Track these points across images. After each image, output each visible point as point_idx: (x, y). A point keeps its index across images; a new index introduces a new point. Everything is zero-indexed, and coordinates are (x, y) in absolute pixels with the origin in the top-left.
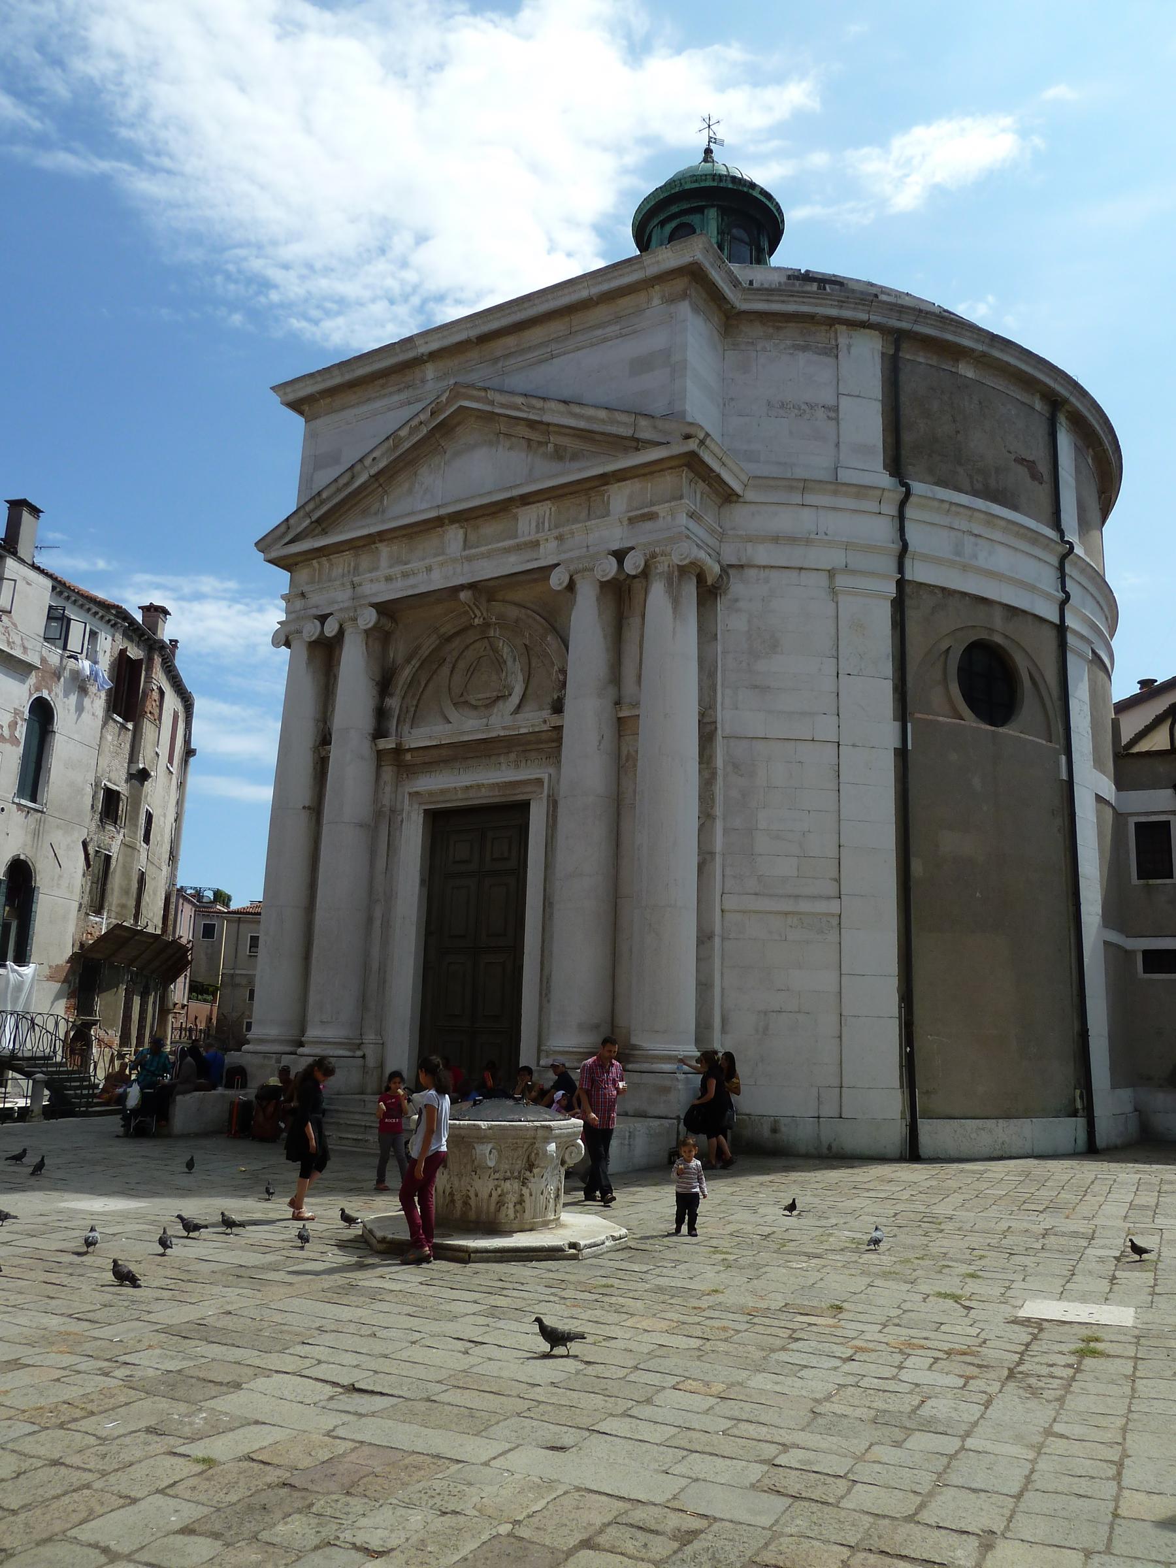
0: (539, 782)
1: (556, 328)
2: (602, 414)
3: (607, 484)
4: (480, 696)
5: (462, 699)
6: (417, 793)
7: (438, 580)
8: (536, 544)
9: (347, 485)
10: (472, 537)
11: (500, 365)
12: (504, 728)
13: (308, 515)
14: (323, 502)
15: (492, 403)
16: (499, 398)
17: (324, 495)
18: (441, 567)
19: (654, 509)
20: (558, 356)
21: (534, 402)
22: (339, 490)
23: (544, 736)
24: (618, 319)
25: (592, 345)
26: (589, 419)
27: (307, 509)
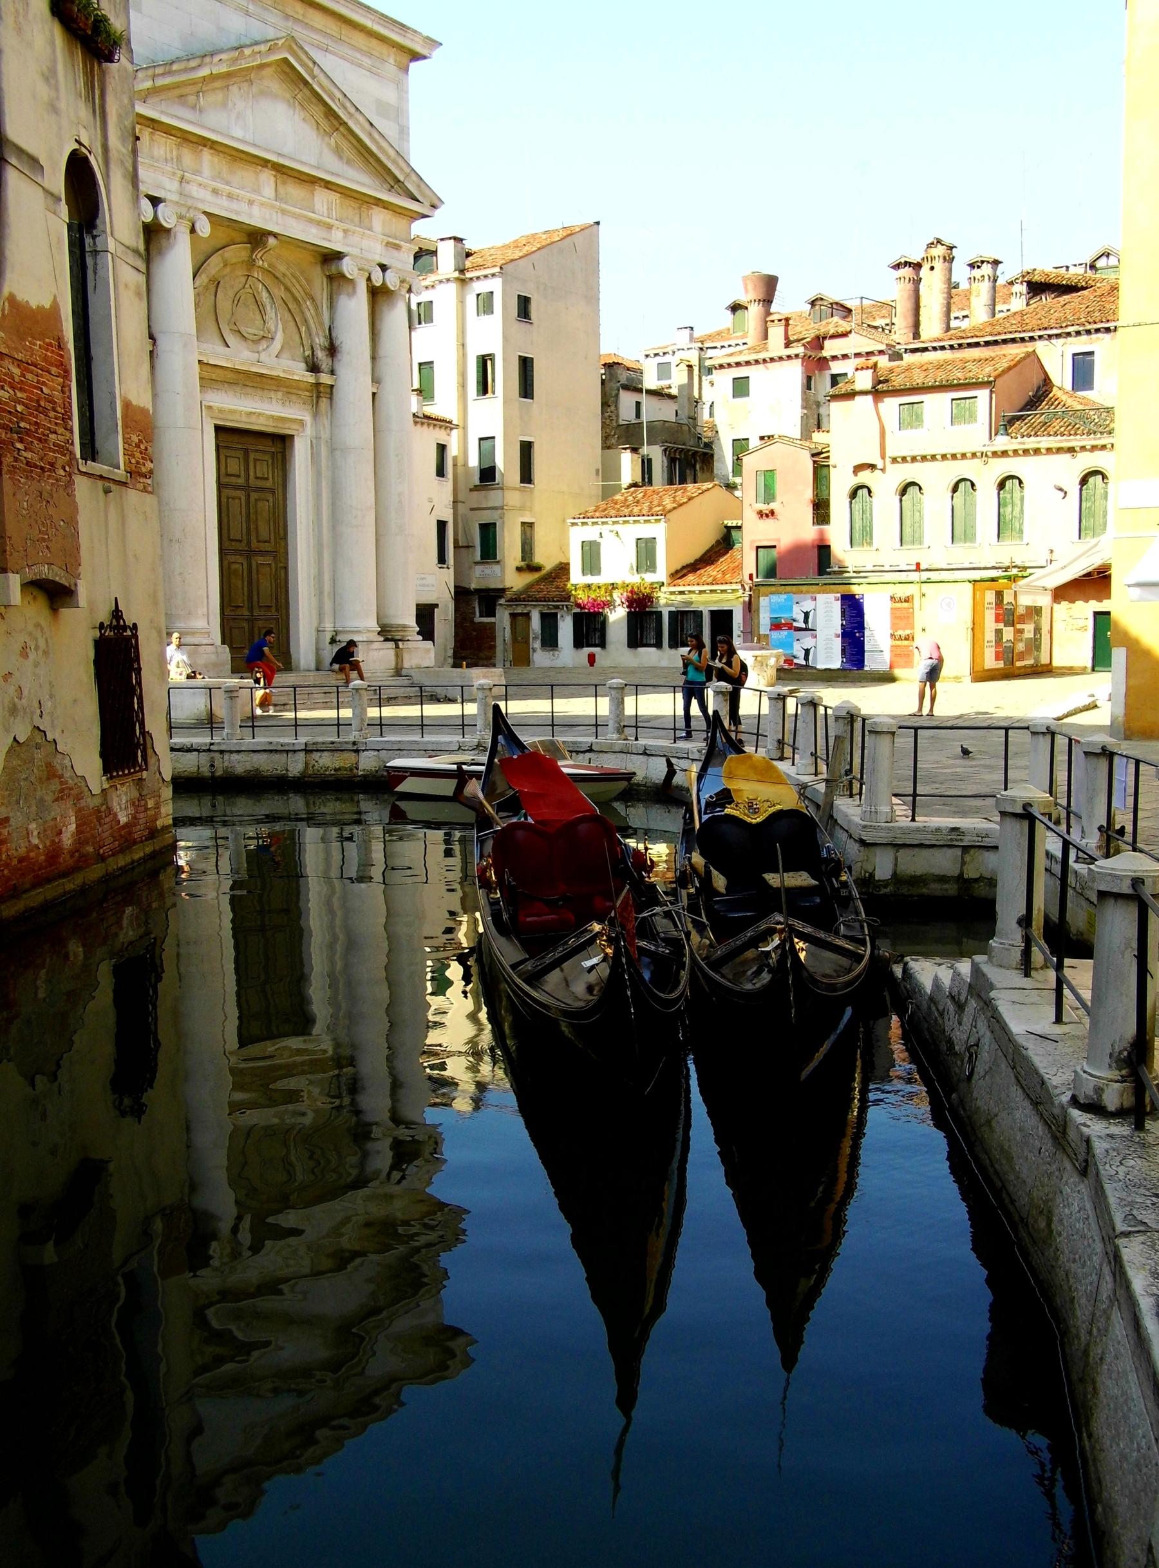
0: (301, 423)
1: (332, 26)
2: (392, 153)
3: (377, 205)
4: (250, 330)
6: (210, 407)
7: (257, 218)
8: (329, 227)
9: (193, 69)
10: (281, 189)
11: (290, 24)
12: (284, 371)
13: (154, 77)
14: (170, 73)
15: (314, 77)
16: (322, 77)
17: (175, 67)
18: (258, 205)
19: (402, 243)
20: (331, 53)
21: (348, 105)
22: (186, 70)
23: (302, 385)
24: (369, 55)
25: (352, 63)
26: (380, 148)
27: (159, 71)
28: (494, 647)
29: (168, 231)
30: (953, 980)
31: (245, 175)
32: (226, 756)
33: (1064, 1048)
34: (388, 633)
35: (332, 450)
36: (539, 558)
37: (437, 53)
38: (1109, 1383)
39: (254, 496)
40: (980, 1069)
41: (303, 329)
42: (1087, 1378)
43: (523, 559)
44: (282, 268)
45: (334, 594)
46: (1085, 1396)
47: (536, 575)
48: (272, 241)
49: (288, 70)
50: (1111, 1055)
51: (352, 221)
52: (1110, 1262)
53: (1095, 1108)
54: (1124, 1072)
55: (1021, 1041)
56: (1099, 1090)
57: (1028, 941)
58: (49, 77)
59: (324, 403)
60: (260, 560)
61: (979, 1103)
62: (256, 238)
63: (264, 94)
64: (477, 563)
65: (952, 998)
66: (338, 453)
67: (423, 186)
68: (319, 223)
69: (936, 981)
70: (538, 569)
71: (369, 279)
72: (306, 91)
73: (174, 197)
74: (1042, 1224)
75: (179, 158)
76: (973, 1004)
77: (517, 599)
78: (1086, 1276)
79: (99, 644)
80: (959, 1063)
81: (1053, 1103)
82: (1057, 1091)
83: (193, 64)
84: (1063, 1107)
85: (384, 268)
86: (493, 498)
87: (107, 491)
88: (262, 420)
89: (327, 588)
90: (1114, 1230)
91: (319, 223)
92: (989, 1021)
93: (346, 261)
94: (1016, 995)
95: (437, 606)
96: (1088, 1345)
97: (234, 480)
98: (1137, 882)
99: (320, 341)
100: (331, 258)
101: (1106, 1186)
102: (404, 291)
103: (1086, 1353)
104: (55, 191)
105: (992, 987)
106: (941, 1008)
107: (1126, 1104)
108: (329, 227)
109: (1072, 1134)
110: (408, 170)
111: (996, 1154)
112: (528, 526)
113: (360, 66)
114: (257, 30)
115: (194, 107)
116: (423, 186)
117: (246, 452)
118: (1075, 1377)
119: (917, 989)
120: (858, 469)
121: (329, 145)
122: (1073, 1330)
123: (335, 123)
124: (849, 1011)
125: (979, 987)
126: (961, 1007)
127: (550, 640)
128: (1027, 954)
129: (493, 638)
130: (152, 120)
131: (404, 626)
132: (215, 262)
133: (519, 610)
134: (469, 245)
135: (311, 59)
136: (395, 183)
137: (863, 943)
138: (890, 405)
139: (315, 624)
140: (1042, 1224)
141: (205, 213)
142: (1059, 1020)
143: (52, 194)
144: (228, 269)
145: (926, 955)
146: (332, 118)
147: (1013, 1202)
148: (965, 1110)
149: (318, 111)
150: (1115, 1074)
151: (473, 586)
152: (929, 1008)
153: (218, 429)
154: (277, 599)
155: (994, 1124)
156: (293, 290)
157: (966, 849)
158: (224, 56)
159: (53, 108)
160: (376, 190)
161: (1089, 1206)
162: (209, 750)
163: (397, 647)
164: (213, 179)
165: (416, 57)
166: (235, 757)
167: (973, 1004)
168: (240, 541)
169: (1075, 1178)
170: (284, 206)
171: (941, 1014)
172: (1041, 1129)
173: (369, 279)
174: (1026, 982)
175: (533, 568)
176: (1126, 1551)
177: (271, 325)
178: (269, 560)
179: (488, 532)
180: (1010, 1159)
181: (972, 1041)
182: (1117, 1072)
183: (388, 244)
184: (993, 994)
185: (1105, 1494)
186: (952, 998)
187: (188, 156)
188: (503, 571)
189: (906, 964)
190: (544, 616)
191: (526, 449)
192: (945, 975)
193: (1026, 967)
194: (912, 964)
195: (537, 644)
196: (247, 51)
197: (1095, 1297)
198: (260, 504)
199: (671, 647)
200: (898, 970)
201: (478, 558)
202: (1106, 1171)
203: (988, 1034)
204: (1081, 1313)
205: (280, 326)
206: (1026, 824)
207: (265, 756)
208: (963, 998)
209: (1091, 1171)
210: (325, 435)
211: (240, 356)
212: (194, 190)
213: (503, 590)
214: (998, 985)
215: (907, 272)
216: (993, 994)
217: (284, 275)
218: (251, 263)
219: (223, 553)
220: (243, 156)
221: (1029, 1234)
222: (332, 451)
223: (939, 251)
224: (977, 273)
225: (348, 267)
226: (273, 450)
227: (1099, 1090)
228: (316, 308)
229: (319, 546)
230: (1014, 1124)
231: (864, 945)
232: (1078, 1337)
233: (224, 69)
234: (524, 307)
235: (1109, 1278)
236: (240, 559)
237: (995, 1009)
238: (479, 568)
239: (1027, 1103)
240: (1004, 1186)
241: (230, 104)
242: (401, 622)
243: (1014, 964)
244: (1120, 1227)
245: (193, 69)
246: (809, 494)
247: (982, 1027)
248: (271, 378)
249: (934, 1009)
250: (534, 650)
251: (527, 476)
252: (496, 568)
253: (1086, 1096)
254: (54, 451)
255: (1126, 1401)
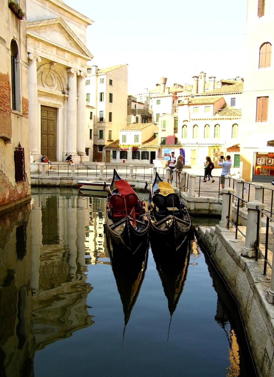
0: (60, 105)
1: (70, 16)
2: (83, 45)
5: (46, 83)
7: (52, 58)
8: (68, 61)
9: (38, 24)
11: (61, 15)
12: (57, 93)
15: (66, 27)
16: (68, 27)
17: (34, 23)
20: (70, 22)
21: (73, 34)
23: (61, 97)
24: (78, 23)
25: (74, 25)
26: (80, 44)
27: (30, 24)
28: (102, 158)
29: (31, 60)
30: (211, 230)
31: (50, 48)
32: (42, 180)
33: (238, 244)
34: (79, 154)
35: (67, 112)
36: (112, 139)
37: (93, 24)
38: (253, 315)
39: (49, 121)
40: (218, 249)
41: (62, 84)
42: (247, 315)
43: (109, 139)
44: (57, 70)
45: (67, 144)
46: (246, 318)
47: (112, 142)
48: (55, 64)
49: (60, 25)
50: (250, 245)
51: (73, 60)
52: (252, 289)
53: (246, 256)
54: (253, 249)
55: (229, 242)
56: (247, 253)
57: (229, 221)
58: (8, 22)
59: (66, 101)
60: (50, 136)
61: (218, 257)
62: (52, 63)
63: (54, 30)
64: (99, 139)
65: (211, 234)
66: (69, 112)
67: (90, 53)
68: (66, 60)
69: (207, 231)
70: (112, 141)
71: (77, 74)
72: (64, 30)
73: (33, 53)
74: (234, 282)
75: (34, 44)
76: (216, 235)
77: (107, 148)
78: (245, 293)
79: (16, 152)
80: (212, 248)
81: (237, 256)
82: (238, 253)
83: (38, 22)
84: (239, 256)
85: (80, 71)
86: (102, 124)
87: (18, 117)
88: (51, 104)
89: (65, 143)
90: (254, 282)
91: (66, 60)
92: (220, 239)
93: (72, 69)
94: (226, 233)
95: (89, 148)
96: (246, 307)
97: (45, 118)
98: (257, 207)
99: (65, 87)
100: (68, 68)
101: (251, 273)
102: (85, 77)
103: (246, 309)
104: (9, 48)
105: (221, 231)
106: (208, 236)
107: (253, 256)
108: (68, 61)
109: (241, 262)
110: (86, 49)
111: (222, 268)
112: (110, 131)
113: (76, 26)
114: (53, 16)
115: (38, 32)
116: (90, 53)
117: (48, 111)
118: (243, 315)
119: (201, 233)
120: (184, 121)
121: (69, 43)
122: (242, 305)
123: (70, 38)
124: (186, 238)
125: (218, 232)
126: (213, 236)
127: (115, 157)
128: (228, 224)
129: (102, 156)
130: (28, 35)
131: (83, 152)
132: (42, 67)
133: (108, 150)
134: (99, 68)
135: (65, 23)
136: (84, 52)
137: (189, 222)
138: (192, 107)
139: (62, 151)
140: (234, 282)
141: (40, 56)
142: (236, 238)
143: (8, 49)
144: (45, 70)
145: (203, 226)
146: (70, 37)
147: (226, 278)
148: (214, 258)
149: (66, 35)
150: (251, 249)
151: (97, 144)
152: (205, 237)
153: (41, 106)
154: (54, 145)
155: (221, 261)
156: (60, 75)
157: (210, 203)
158: (45, 21)
159: (8, 29)
160: (79, 53)
161: (246, 277)
162: (38, 178)
163: (81, 157)
164: (42, 49)
165: (89, 24)
166: (44, 180)
167: (216, 235)
168: (46, 131)
169: (242, 272)
170: (58, 56)
171: (208, 238)
172: (233, 261)
173: (77, 74)
174: (228, 230)
175: (111, 141)
176: (259, 351)
177: (54, 83)
178: (52, 136)
179: (101, 132)
180: (225, 268)
181: (216, 243)
182: (251, 249)
183: (81, 66)
184: (221, 233)
185: (252, 339)
186: (211, 234)
187: (36, 43)
188: (104, 141)
189: (199, 227)
190: (113, 151)
191: (110, 114)
192: (209, 230)
193: (228, 227)
194: (200, 227)
195: (112, 158)
196: (51, 20)
197: (248, 297)
198: (51, 123)
199: (142, 159)
200: (197, 229)
201: (99, 138)
202: (250, 270)
203: (220, 241)
204: (244, 301)
205: (56, 83)
206: (229, 196)
207: (51, 180)
208: (213, 234)
209: (247, 270)
210: (66, 108)
211: (47, 89)
212: (37, 51)
213: (104, 145)
214: (222, 231)
215: (196, 79)
216: (221, 233)
217: (58, 72)
218: (50, 69)
219: (42, 134)
220: (49, 44)
221: (230, 285)
222: (67, 112)
223: (203, 74)
224: (210, 79)
225: (72, 70)
226: (54, 111)
227: (247, 253)
228: (65, 79)
229: (64, 134)
230: (226, 262)
231: (190, 223)
232: (243, 306)
233: (45, 24)
234: (111, 82)
235: (252, 293)
236: (46, 136)
237: (222, 236)
238: (99, 140)
239: (230, 256)
240: (224, 275)
241: (46, 32)
242: (82, 151)
243: (225, 227)
244: (255, 281)
245: (38, 24)
246: (173, 127)
247: (218, 240)
248: (54, 95)
249: (206, 237)
250: (111, 159)
251: (110, 120)
252: (103, 140)
253: (244, 254)
254: (7, 107)
255: (258, 318)
